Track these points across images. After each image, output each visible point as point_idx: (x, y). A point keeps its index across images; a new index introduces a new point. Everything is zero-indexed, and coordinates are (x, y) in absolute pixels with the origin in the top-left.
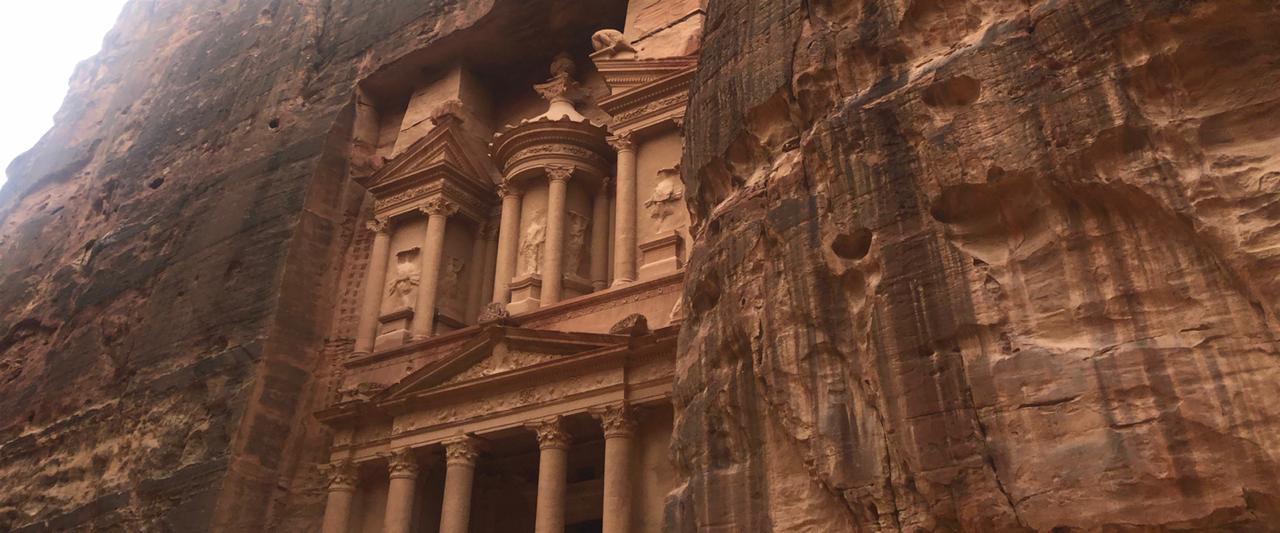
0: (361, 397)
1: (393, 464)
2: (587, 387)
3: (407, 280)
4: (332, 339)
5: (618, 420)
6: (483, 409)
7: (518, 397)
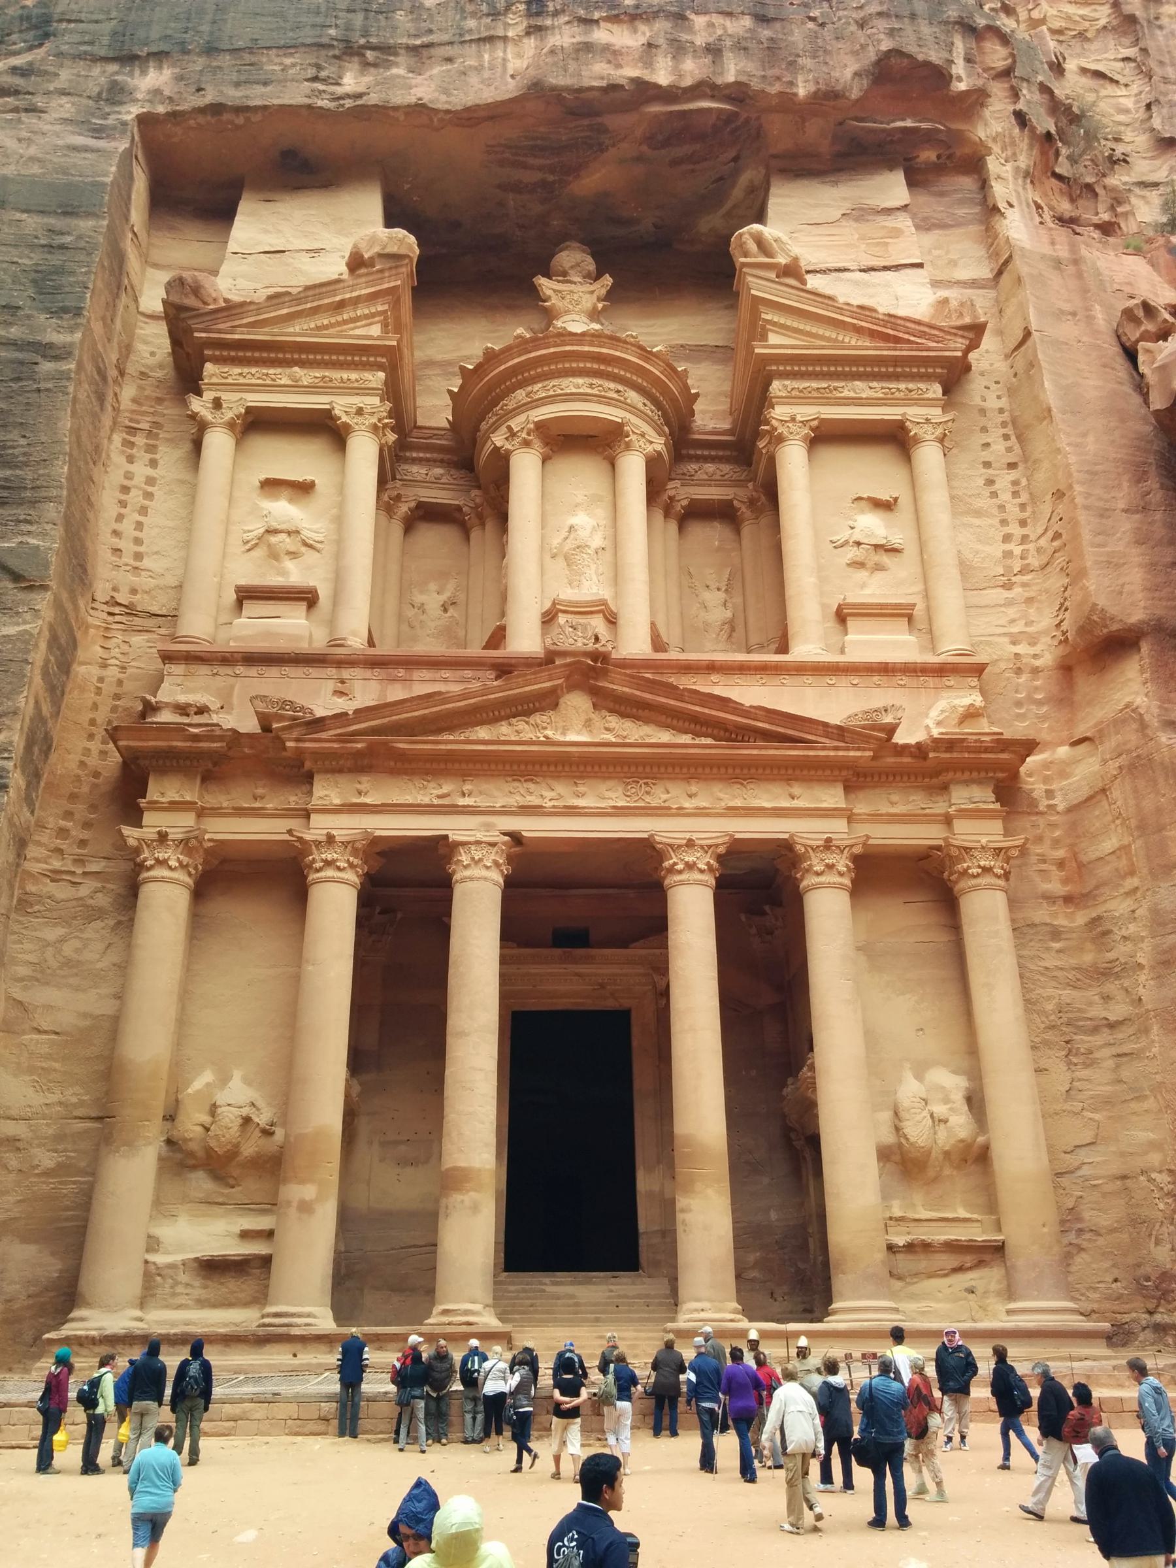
0: (215, 719)
1: (329, 857)
3: (293, 533)
4: (102, 596)
5: (842, 863)
6: (547, 794)
7: (620, 789)
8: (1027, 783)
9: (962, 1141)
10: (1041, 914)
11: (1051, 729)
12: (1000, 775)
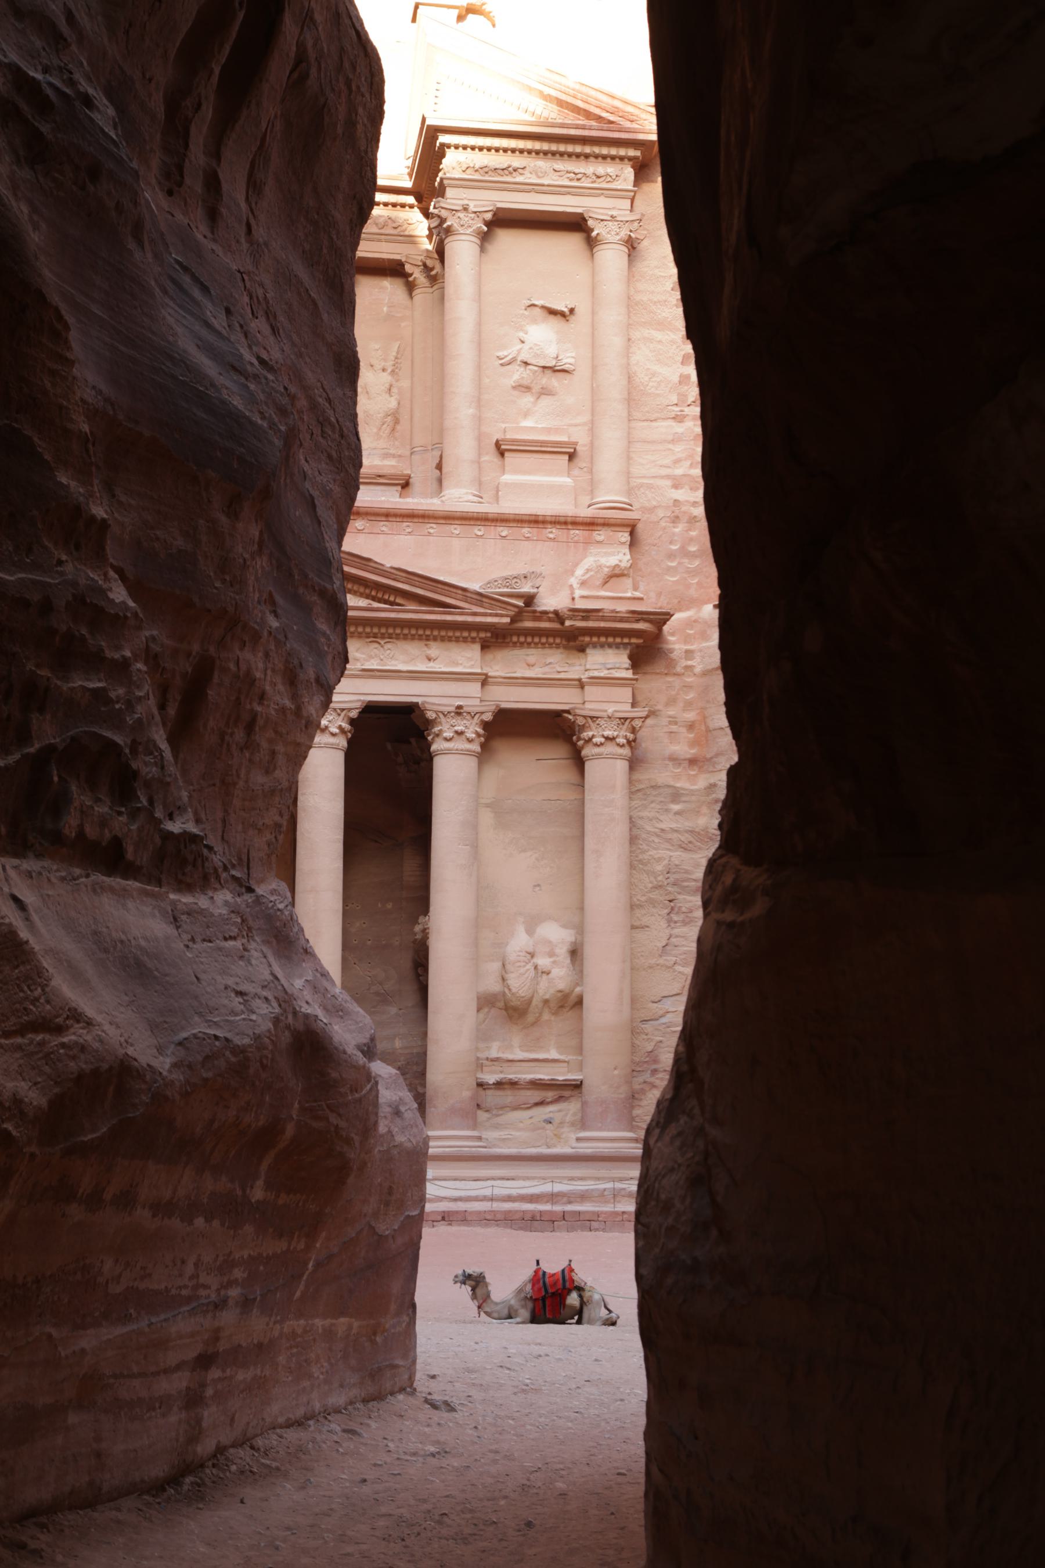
2: (404, 662)
5: (472, 728)
8: (667, 642)
9: (560, 991)
10: (663, 775)
11: (697, 583)
12: (634, 640)
